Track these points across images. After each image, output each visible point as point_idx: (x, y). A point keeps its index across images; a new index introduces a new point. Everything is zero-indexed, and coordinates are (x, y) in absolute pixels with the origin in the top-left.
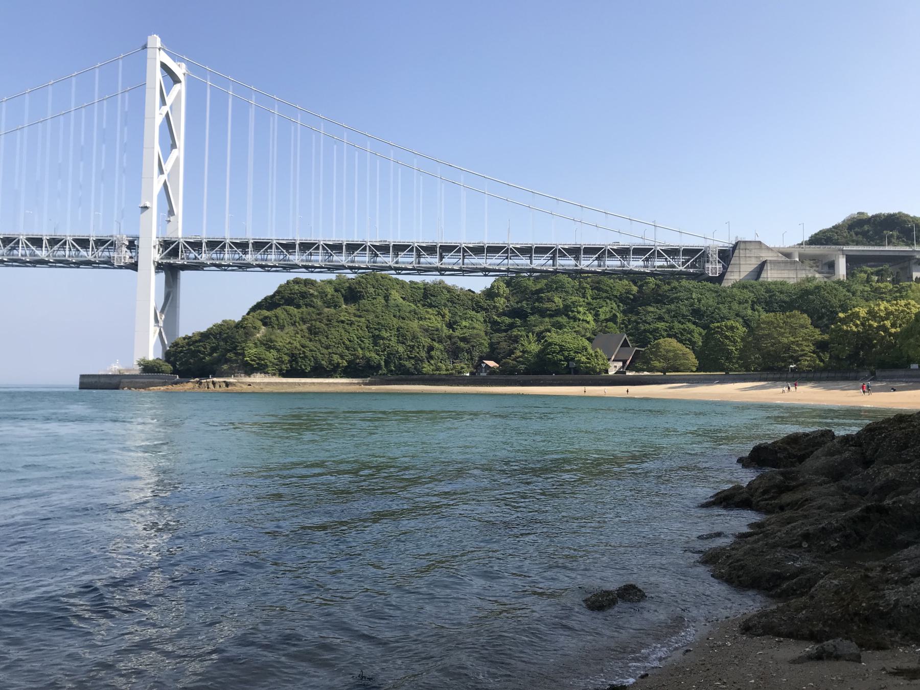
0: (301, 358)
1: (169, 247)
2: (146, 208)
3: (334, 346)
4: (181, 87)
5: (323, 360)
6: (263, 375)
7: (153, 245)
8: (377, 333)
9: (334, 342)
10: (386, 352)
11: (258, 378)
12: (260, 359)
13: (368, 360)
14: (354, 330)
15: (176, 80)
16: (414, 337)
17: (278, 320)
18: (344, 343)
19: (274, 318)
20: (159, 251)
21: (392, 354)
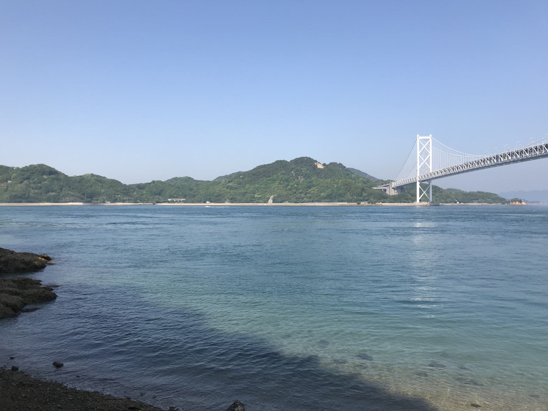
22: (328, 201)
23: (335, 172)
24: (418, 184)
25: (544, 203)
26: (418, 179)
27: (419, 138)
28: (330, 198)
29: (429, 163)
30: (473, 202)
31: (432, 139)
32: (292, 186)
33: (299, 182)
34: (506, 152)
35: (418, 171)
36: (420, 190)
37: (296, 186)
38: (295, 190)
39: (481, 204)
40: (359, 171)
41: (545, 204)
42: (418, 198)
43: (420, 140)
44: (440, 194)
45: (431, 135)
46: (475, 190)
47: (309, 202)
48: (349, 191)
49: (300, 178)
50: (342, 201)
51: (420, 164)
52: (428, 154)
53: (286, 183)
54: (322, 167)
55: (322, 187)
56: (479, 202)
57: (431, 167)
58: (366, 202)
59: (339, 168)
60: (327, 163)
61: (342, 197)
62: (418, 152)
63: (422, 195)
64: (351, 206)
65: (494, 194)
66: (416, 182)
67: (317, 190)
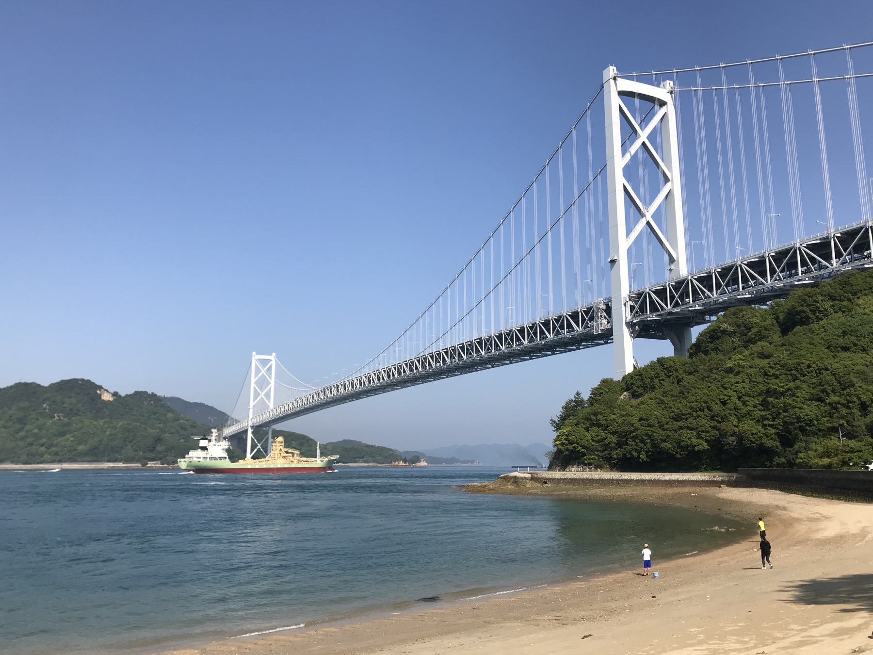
0: (631, 438)
1: (639, 301)
2: (613, 262)
3: (693, 416)
4: (667, 109)
5: (665, 441)
7: (623, 303)
8: (775, 385)
10: (777, 421)
11: (574, 473)
13: (741, 438)
14: (737, 383)
15: (662, 103)
16: (846, 386)
18: (709, 408)
19: (637, 378)
20: (632, 308)
21: (792, 424)
23: (132, 409)
24: (250, 431)
25: (479, 462)
26: (250, 424)
27: (256, 357)
28: (94, 455)
29: (269, 399)
31: (276, 360)
34: (332, 384)
35: (251, 411)
36: (252, 440)
37: (36, 431)
38: (33, 439)
39: (367, 464)
40: (212, 408)
41: (480, 464)
42: (249, 455)
43: (256, 360)
44: (307, 448)
45: (274, 354)
46: (377, 444)
47: (53, 462)
48: (131, 442)
49: (59, 416)
50: (115, 461)
51: (254, 400)
52: (269, 383)
53: (18, 426)
54: (111, 399)
55: (84, 433)
56: (365, 462)
57: (271, 406)
58: (159, 462)
60: (123, 395)
61: (116, 452)
62: (253, 380)
63: (256, 450)
64: (129, 469)
65: (388, 448)
66: (246, 431)
67: (72, 439)
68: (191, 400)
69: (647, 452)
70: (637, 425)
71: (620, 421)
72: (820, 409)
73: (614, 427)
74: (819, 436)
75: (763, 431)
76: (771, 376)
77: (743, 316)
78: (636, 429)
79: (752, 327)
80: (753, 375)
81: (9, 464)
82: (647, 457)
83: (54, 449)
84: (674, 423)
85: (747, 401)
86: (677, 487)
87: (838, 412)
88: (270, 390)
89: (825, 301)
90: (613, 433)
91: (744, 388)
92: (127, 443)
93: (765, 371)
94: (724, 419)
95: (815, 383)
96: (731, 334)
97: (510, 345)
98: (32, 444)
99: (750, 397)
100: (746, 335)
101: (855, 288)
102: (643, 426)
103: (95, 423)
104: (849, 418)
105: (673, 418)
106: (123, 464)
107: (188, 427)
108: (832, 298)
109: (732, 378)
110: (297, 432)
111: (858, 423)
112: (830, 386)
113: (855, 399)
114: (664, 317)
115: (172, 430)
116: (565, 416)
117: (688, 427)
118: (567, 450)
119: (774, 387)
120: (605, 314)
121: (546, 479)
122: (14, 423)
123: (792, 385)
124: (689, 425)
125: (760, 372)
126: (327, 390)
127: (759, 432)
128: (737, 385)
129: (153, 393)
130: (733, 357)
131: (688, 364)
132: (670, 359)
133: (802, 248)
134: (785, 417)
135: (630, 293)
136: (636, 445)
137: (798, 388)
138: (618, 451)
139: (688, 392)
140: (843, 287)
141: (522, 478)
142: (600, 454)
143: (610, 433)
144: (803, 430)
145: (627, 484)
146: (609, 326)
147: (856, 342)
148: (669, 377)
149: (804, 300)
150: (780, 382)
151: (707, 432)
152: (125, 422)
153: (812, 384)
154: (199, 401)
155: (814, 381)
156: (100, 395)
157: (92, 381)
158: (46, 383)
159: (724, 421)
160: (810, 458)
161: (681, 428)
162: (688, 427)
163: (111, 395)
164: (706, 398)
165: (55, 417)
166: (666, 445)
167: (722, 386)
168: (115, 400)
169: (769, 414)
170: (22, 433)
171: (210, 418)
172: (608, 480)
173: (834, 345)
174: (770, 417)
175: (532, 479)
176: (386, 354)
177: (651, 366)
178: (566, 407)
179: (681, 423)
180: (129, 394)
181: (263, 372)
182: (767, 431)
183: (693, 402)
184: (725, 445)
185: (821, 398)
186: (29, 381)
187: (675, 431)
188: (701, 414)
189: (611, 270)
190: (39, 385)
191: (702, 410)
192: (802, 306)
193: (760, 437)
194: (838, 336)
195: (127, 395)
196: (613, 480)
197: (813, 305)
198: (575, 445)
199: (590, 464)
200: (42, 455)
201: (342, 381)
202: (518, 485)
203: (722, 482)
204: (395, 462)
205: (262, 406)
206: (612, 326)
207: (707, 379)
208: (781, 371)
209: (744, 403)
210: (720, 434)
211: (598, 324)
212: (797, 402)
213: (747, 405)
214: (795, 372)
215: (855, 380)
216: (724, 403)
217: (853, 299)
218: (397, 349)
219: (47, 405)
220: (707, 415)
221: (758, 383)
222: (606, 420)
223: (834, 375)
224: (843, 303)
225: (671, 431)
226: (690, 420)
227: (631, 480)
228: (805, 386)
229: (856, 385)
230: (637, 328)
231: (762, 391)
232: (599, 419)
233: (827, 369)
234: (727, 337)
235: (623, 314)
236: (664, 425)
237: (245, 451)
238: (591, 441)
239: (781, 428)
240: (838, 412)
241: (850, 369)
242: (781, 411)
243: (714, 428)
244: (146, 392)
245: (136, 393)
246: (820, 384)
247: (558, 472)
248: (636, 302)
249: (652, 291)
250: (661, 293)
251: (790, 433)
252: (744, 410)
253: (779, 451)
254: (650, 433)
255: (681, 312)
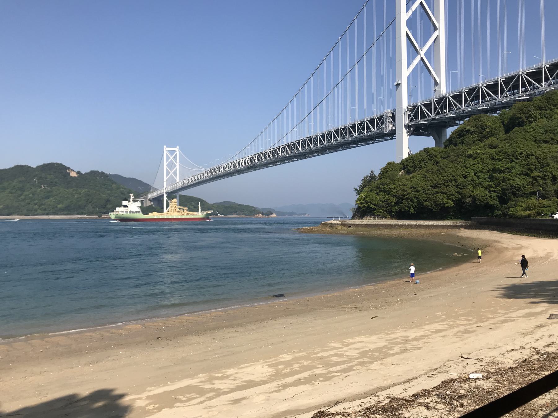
1: (414, 111)
3: (445, 185)
5: (426, 201)
6: (372, 218)
8: (499, 165)
9: (444, 180)
11: (368, 221)
12: (367, 202)
13: (474, 199)
14: (474, 164)
16: (543, 165)
17: (414, 162)
18: (455, 180)
20: (409, 116)
22: (65, 213)
24: (165, 196)
25: (309, 215)
26: (165, 191)
27: (166, 149)
28: (68, 210)
29: (176, 175)
30: (232, 215)
31: (179, 151)
32: (26, 196)
33: (36, 191)
34: (215, 166)
35: (165, 183)
37: (31, 195)
40: (140, 181)
45: (178, 147)
47: (43, 214)
48: (90, 202)
50: (82, 214)
51: (167, 177)
52: (175, 166)
53: (19, 192)
54: (76, 176)
55: (61, 197)
57: (178, 180)
59: (101, 177)
60: (83, 173)
62: (165, 164)
64: (90, 219)
66: (163, 195)
67: (54, 200)
68: (127, 176)
69: (414, 208)
70: (409, 191)
71: (398, 188)
72: (526, 180)
73: (394, 193)
74: (524, 197)
75: (489, 194)
76: (496, 160)
77: (481, 121)
78: (408, 194)
79: (486, 128)
80: (485, 159)
81: (16, 216)
82: (415, 210)
83: (43, 207)
84: (433, 189)
85: (480, 176)
86: (432, 229)
87: (538, 182)
88: (176, 170)
89: (536, 111)
90: (394, 196)
91: (478, 167)
92: (88, 203)
93: (492, 157)
94: (465, 187)
95: (524, 164)
96: (472, 133)
97: (315, 144)
98: (29, 204)
99: (482, 173)
100: (482, 133)
101: (555, 101)
102: (413, 191)
103: (67, 190)
104: (545, 186)
105: (432, 187)
106: (87, 216)
107: (125, 193)
108: (540, 108)
109: (471, 161)
110: (195, 196)
111: (550, 189)
112: (534, 166)
113: (549, 174)
114: (430, 122)
115: (116, 195)
116: (364, 186)
117: (441, 192)
118: (364, 207)
119: (498, 166)
120: (392, 120)
121: (350, 224)
122: (17, 190)
123: (509, 165)
124: (442, 191)
125: (490, 157)
126: (212, 170)
127: (486, 195)
128: (474, 165)
129: (102, 172)
130: (473, 147)
131: (443, 152)
132: (432, 149)
133: (523, 75)
134: (503, 185)
135: (408, 106)
136: (408, 204)
137: (513, 167)
138: (396, 207)
139: (443, 170)
140: (548, 101)
141: (335, 224)
142: (385, 209)
143: (392, 196)
144: (514, 194)
145: (402, 227)
146: (394, 128)
147: (553, 137)
148: (431, 160)
149: (522, 110)
150: (502, 164)
151: (454, 195)
152: (86, 190)
153: (522, 164)
154: (132, 177)
155: (524, 162)
156: (69, 173)
157: (63, 164)
158: (34, 166)
159: (464, 188)
160: (517, 211)
161: (437, 193)
162: (441, 192)
163: (76, 173)
164: (454, 174)
165: (42, 187)
166: (425, 203)
167: (465, 166)
168: (78, 176)
169: (494, 184)
170: (23, 197)
171: (139, 187)
172: (389, 225)
173: (539, 139)
174: (494, 186)
175: (342, 224)
176: (249, 147)
177: (420, 154)
178: (364, 180)
179: (437, 190)
180: (87, 172)
181: (171, 158)
182: (491, 194)
183: (445, 177)
184: (464, 203)
185: (528, 173)
186: (23, 164)
187: (433, 195)
188: (450, 184)
189: (397, 90)
190: (30, 167)
191: (451, 181)
192: (520, 114)
193: (487, 199)
194: (542, 134)
195: (86, 173)
196: (392, 225)
197: (528, 113)
198: (370, 204)
199: (378, 215)
200: (36, 210)
201: (222, 165)
202: (333, 228)
203: (461, 226)
204: (256, 215)
205: (172, 180)
206: (395, 128)
207: (455, 162)
208: (503, 156)
209: (478, 177)
210: (462, 197)
211: (387, 127)
212: (512, 176)
213: (480, 179)
214: (512, 157)
215: (550, 162)
216: (465, 177)
217: (554, 109)
218: (256, 144)
219: (36, 179)
220: (454, 184)
221: (487, 164)
222: (390, 188)
223: (537, 159)
224: (547, 112)
225: (430, 194)
226: (443, 187)
227: (404, 225)
228: (517, 166)
229: (551, 165)
230: (412, 129)
231: (490, 169)
232: (385, 188)
233: (532, 155)
234: (470, 135)
235: (403, 120)
236: (426, 191)
237: (163, 208)
238: (379, 201)
239: (500, 192)
240: (538, 182)
241: (547, 155)
242: (501, 182)
243: (458, 192)
244: (98, 171)
245: (92, 172)
246: (528, 165)
247: (358, 220)
248: (412, 112)
249: (422, 105)
250: (428, 106)
251: (506, 195)
252: (478, 182)
253: (498, 207)
254: (417, 196)
255: (441, 118)
